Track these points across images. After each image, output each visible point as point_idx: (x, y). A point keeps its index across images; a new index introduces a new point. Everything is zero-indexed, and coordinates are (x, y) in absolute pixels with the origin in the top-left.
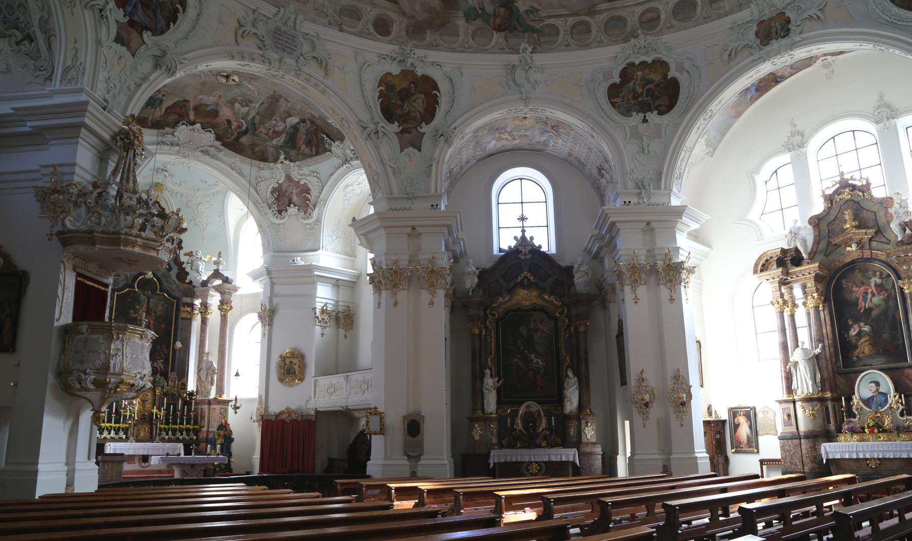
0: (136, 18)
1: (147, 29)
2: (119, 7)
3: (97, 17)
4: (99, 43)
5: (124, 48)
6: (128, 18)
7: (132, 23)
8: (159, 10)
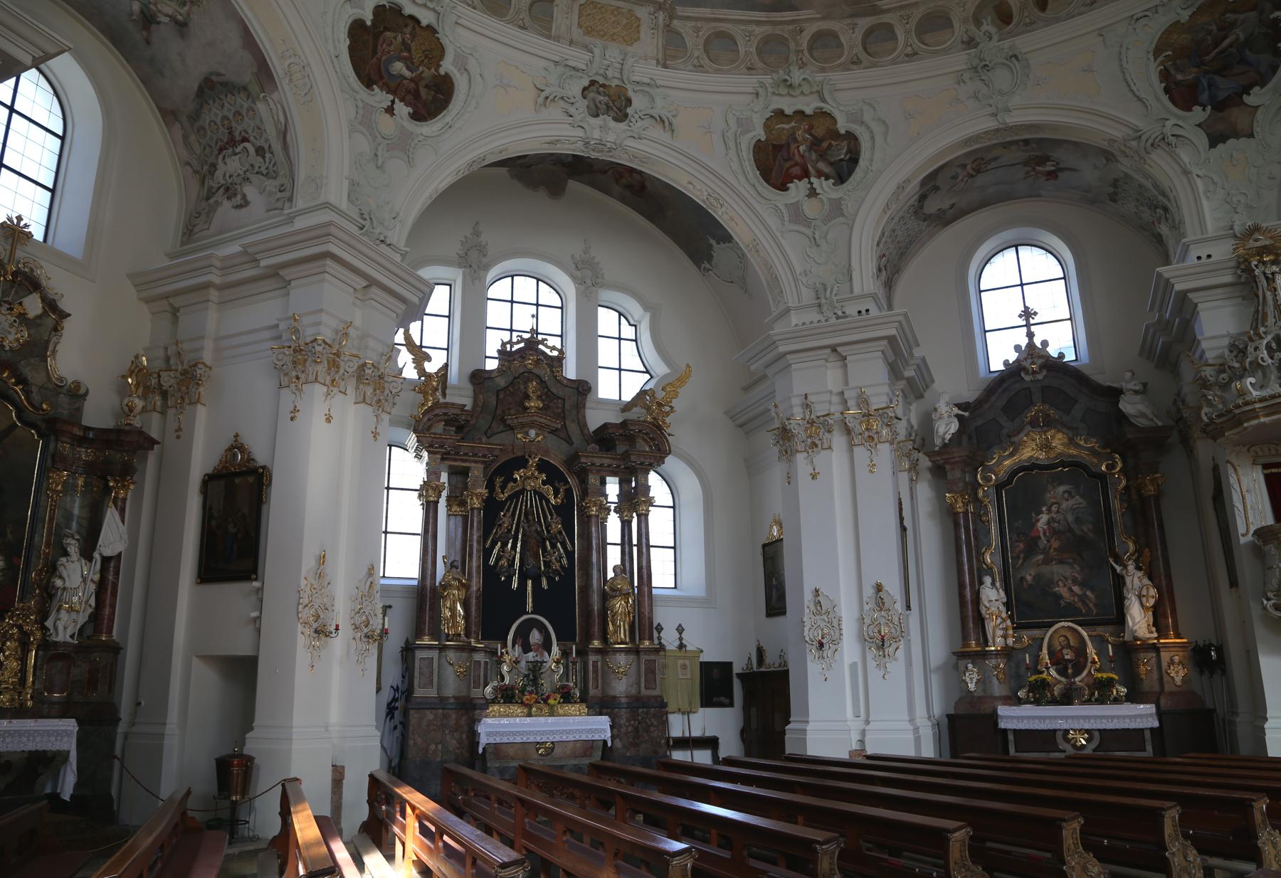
0: (1222, 95)
1: (1247, 90)
2: (1189, 109)
3: (1166, 149)
4: (1186, 172)
5: (1231, 142)
6: (1209, 108)
7: (1219, 106)
8: (1248, 52)
